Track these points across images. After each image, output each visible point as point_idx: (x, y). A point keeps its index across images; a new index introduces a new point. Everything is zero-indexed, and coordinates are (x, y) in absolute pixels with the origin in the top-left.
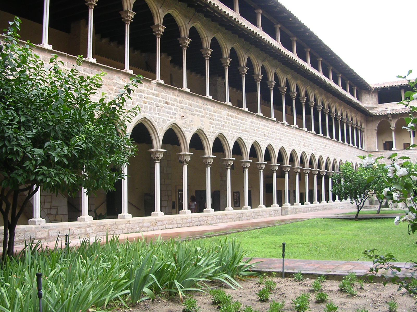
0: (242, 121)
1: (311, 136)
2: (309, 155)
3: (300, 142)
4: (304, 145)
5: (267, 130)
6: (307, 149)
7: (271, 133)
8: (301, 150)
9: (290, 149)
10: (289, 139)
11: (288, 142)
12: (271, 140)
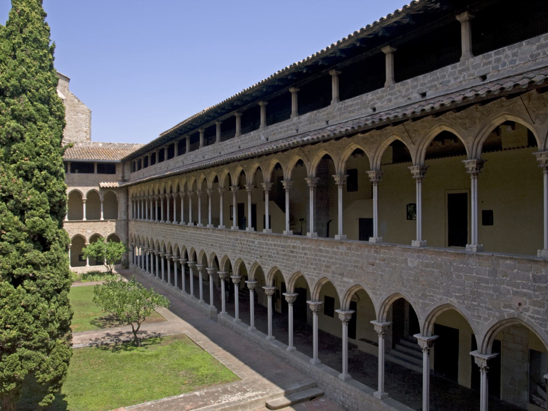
1: (254, 238)
2: (249, 264)
3: (236, 246)
4: (241, 251)
5: (201, 237)
6: (247, 255)
7: (204, 239)
8: (235, 257)
9: (222, 254)
10: (220, 244)
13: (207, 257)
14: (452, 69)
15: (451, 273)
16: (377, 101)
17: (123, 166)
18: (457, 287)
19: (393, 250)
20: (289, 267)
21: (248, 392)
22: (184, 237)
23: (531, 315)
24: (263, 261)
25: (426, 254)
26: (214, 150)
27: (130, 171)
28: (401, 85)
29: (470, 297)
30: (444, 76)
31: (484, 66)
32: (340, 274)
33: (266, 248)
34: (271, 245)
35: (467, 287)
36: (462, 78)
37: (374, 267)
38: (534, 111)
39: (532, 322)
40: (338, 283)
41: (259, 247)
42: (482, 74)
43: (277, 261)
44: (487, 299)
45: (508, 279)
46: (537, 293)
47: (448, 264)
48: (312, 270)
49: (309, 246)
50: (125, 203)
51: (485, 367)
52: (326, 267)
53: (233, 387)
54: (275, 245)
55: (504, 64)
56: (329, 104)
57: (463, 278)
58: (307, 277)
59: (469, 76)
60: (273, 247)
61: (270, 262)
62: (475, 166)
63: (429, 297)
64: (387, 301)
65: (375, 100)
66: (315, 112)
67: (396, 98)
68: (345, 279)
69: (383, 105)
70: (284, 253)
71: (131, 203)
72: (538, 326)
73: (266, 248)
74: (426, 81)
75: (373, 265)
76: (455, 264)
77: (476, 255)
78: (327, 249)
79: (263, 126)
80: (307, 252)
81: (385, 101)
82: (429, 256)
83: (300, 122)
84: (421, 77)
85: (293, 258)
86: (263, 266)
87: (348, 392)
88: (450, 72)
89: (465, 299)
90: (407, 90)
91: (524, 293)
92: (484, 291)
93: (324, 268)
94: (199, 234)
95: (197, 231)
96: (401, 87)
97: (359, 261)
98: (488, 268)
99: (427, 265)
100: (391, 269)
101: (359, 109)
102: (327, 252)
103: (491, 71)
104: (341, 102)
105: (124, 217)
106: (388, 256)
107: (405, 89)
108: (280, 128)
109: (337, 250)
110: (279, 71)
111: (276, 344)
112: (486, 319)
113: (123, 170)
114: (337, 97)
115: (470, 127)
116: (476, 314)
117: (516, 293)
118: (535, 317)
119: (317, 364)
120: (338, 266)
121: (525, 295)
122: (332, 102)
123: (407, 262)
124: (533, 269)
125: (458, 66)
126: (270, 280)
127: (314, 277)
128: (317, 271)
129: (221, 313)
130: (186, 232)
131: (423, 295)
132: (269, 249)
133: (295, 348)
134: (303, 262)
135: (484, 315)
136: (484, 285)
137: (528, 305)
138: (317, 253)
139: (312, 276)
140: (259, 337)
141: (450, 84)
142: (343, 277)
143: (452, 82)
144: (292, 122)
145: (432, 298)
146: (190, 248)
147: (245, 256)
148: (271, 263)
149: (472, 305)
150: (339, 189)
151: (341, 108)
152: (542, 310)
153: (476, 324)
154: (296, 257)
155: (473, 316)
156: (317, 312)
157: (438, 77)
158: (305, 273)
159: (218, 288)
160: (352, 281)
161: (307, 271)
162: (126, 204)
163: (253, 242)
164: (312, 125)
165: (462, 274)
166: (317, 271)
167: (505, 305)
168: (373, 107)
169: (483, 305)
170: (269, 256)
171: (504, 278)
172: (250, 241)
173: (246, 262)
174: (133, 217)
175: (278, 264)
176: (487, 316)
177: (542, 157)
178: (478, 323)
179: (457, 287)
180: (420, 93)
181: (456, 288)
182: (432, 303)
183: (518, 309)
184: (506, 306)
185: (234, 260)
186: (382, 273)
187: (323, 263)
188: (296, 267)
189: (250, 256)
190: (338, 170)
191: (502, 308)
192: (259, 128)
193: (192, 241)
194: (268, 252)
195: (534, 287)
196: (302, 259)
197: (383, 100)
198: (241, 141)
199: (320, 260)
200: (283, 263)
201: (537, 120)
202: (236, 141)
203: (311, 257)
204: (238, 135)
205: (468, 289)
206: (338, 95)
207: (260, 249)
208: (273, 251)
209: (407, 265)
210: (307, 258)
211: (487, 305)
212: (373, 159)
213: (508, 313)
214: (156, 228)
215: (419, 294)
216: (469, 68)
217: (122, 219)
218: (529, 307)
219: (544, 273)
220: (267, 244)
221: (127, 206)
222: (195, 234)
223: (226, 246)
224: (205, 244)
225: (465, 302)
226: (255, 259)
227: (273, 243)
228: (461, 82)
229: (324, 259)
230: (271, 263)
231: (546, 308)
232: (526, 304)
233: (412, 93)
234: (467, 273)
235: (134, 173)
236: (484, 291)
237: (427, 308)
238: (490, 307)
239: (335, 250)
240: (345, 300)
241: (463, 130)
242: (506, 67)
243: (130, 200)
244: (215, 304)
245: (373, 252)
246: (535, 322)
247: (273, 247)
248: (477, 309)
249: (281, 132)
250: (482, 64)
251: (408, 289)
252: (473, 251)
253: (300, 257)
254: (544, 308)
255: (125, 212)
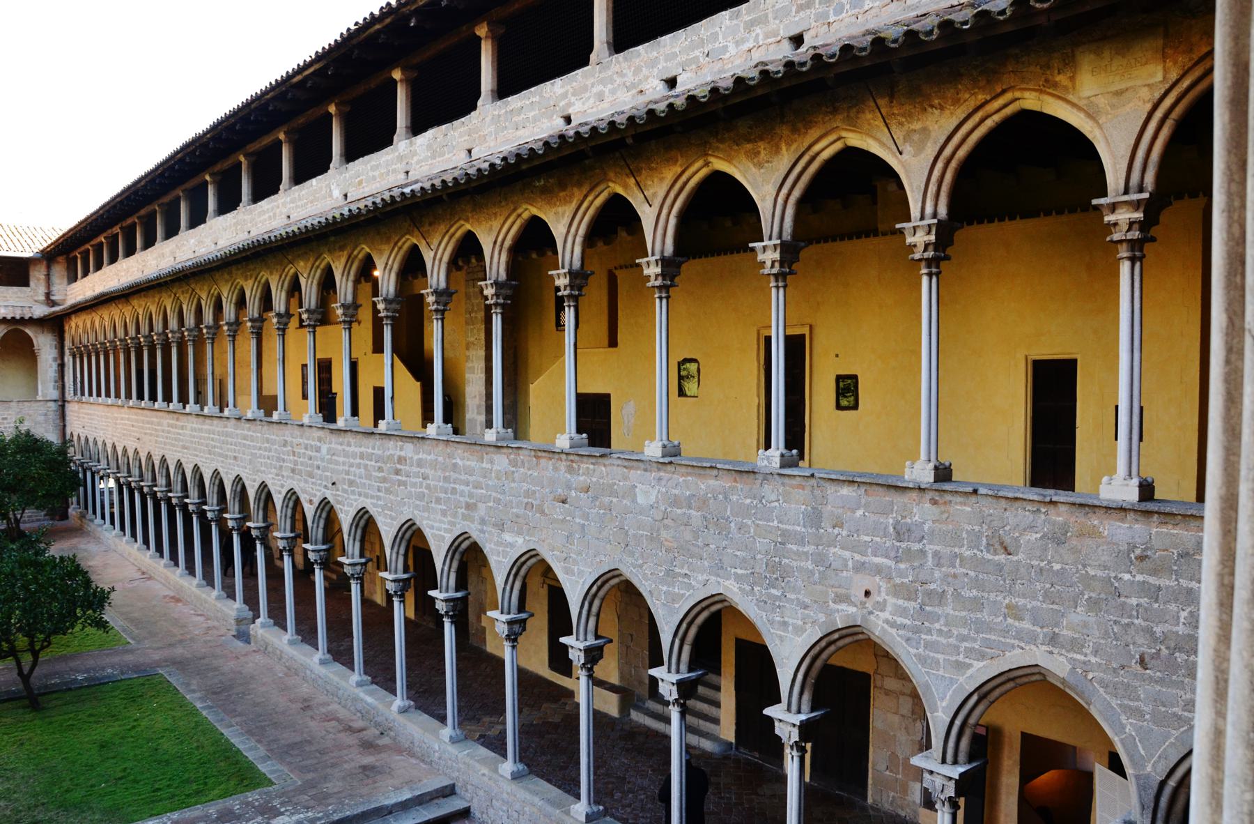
0: (181, 431)
1: (320, 440)
2: (311, 502)
3: (284, 460)
4: (293, 471)
5: (213, 440)
6: (306, 481)
8: (282, 486)
10: (252, 454)
11: (251, 462)
12: (218, 461)
13: (226, 487)
14: (731, 19)
15: (727, 521)
16: (573, 99)
17: (49, 268)
18: (738, 553)
19: (605, 466)
20: (391, 509)
21: (282, 814)
22: (179, 440)
23: (890, 617)
24: (339, 495)
25: (674, 473)
26: (236, 224)
27: (65, 281)
28: (626, 59)
29: (766, 577)
30: (715, 37)
31: (797, 12)
32: (495, 525)
33: (344, 464)
34: (354, 455)
35: (759, 552)
36: (752, 41)
37: (567, 506)
38: (901, 124)
39: (891, 634)
40: (492, 546)
41: (330, 461)
42: (795, 31)
43: (366, 496)
44: (800, 583)
45: (844, 533)
46: (902, 566)
47: (720, 496)
48: (439, 517)
49: (432, 457)
50: (55, 360)
51: (796, 742)
52: (469, 506)
53: (248, 804)
54: (362, 456)
55: (840, 9)
56: (474, 108)
57: (752, 530)
58: (428, 533)
59: (767, 36)
60: (358, 461)
61: (352, 497)
62: (777, 256)
63: (680, 579)
64: (595, 588)
65: (569, 96)
66: (444, 126)
67: (613, 92)
68: (508, 537)
69: (586, 108)
70: (381, 475)
71: (71, 359)
72: (904, 643)
73: (344, 464)
74: (677, 50)
75: (564, 502)
76: (734, 498)
77: (779, 474)
78: (468, 463)
79: (337, 165)
80: (427, 471)
81: (589, 98)
82: (681, 480)
83: (414, 154)
84: (666, 39)
85: (399, 486)
86: (338, 506)
87: (517, 807)
88: (727, 27)
89: (754, 583)
90: (638, 70)
91: (877, 565)
92: (794, 564)
93: (463, 510)
94: (209, 432)
95: (203, 423)
96: (625, 65)
97: (534, 492)
98: (804, 507)
99: (675, 502)
100: (602, 512)
101: (535, 120)
102: (470, 472)
103: (813, 24)
104: (499, 103)
105: (55, 394)
106: (594, 480)
107: (633, 69)
108: (373, 169)
109: (489, 466)
110: (356, 24)
111: (371, 694)
112: (799, 630)
113: (48, 276)
114: (492, 91)
115: (768, 162)
116: (778, 618)
117: (860, 567)
118: (899, 623)
119: (453, 741)
120: (491, 504)
121: (878, 570)
122: (480, 103)
123: (635, 495)
124: (896, 508)
125: (744, 12)
126: (354, 540)
127: (442, 533)
128: (449, 518)
129: (258, 621)
130: (182, 428)
131: (669, 572)
132: (351, 465)
133: (412, 703)
134: (421, 497)
135: (795, 621)
136: (794, 548)
137: (883, 594)
138: (447, 474)
139: (439, 530)
140: (336, 679)
141: (728, 55)
142: (503, 531)
143: (732, 50)
144: (397, 154)
145: (686, 580)
146: (192, 466)
147: (302, 484)
148: (356, 500)
149: (769, 596)
150: (494, 316)
151: (499, 116)
152: (912, 605)
153: (777, 642)
154: (404, 484)
155: (772, 622)
156: (451, 617)
157: (703, 40)
158: (425, 522)
159: (278, 563)
160: (520, 540)
161: (428, 518)
162: (59, 362)
163: (318, 450)
164: (438, 159)
165: (749, 522)
166: (449, 518)
167: (837, 595)
168: (565, 114)
169: (793, 596)
170: (351, 483)
171: (836, 531)
172: (312, 446)
173: (305, 498)
174: (75, 394)
175: (369, 501)
176: (800, 623)
177: (917, 235)
178: (781, 638)
179: (738, 553)
180: (664, 78)
181: (736, 556)
182: (688, 594)
183: (863, 604)
184: (840, 599)
185: (280, 493)
186: (582, 522)
187: (461, 499)
188: (406, 508)
189: (313, 483)
190: (490, 268)
191: (830, 602)
192: (329, 168)
193: (195, 449)
194: (348, 473)
195: (898, 552)
196: (418, 490)
197: (587, 95)
198: (292, 202)
199: (454, 491)
200: (379, 498)
201: (907, 144)
202: (281, 201)
203: (437, 483)
204: (287, 187)
205: (761, 559)
206: (495, 84)
207: (332, 466)
208: (358, 471)
209: (634, 500)
210: (428, 487)
211: (801, 597)
212: (565, 242)
213: (843, 615)
214: (122, 419)
215: (661, 571)
216: (766, 16)
217: (48, 398)
218: (885, 601)
219: (917, 518)
220: (346, 455)
221: (62, 366)
222: (201, 430)
223: (262, 460)
224: (220, 455)
225: (756, 589)
226: (323, 490)
227: (358, 450)
228: (750, 51)
229: (463, 487)
230: (356, 500)
231: (919, 601)
232: (880, 592)
233: (647, 78)
234: (760, 520)
235: (74, 285)
236: (794, 564)
237: (677, 606)
238: (806, 600)
239: (484, 465)
240: (508, 588)
241: (754, 169)
242: (844, 15)
243: (67, 352)
244: (246, 601)
245: (563, 469)
246: (898, 635)
247: (358, 461)
248: (779, 607)
249: (374, 178)
250: (794, 9)
251: (637, 560)
252: (774, 465)
253: (414, 485)
254: (916, 601)
255: (56, 382)
